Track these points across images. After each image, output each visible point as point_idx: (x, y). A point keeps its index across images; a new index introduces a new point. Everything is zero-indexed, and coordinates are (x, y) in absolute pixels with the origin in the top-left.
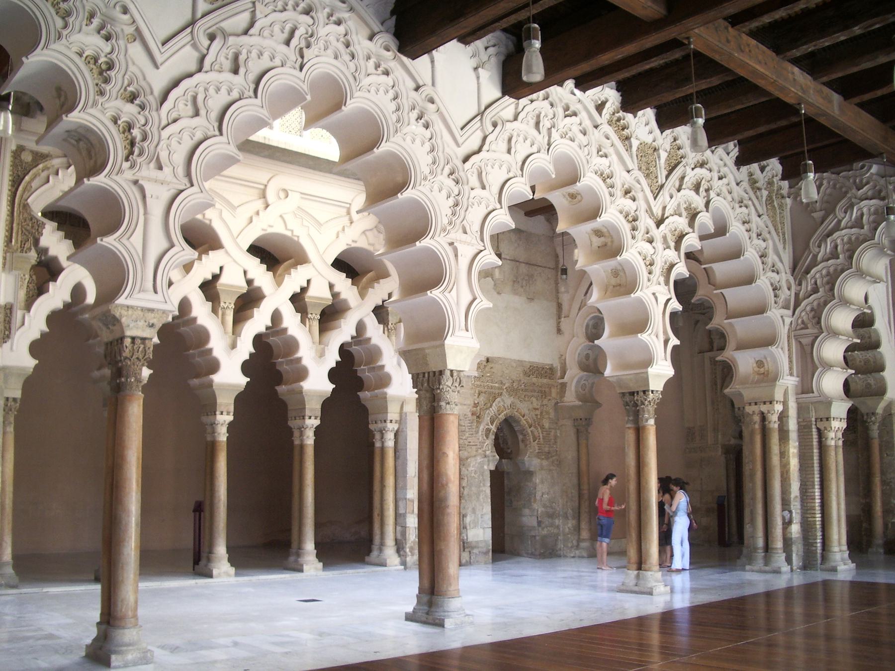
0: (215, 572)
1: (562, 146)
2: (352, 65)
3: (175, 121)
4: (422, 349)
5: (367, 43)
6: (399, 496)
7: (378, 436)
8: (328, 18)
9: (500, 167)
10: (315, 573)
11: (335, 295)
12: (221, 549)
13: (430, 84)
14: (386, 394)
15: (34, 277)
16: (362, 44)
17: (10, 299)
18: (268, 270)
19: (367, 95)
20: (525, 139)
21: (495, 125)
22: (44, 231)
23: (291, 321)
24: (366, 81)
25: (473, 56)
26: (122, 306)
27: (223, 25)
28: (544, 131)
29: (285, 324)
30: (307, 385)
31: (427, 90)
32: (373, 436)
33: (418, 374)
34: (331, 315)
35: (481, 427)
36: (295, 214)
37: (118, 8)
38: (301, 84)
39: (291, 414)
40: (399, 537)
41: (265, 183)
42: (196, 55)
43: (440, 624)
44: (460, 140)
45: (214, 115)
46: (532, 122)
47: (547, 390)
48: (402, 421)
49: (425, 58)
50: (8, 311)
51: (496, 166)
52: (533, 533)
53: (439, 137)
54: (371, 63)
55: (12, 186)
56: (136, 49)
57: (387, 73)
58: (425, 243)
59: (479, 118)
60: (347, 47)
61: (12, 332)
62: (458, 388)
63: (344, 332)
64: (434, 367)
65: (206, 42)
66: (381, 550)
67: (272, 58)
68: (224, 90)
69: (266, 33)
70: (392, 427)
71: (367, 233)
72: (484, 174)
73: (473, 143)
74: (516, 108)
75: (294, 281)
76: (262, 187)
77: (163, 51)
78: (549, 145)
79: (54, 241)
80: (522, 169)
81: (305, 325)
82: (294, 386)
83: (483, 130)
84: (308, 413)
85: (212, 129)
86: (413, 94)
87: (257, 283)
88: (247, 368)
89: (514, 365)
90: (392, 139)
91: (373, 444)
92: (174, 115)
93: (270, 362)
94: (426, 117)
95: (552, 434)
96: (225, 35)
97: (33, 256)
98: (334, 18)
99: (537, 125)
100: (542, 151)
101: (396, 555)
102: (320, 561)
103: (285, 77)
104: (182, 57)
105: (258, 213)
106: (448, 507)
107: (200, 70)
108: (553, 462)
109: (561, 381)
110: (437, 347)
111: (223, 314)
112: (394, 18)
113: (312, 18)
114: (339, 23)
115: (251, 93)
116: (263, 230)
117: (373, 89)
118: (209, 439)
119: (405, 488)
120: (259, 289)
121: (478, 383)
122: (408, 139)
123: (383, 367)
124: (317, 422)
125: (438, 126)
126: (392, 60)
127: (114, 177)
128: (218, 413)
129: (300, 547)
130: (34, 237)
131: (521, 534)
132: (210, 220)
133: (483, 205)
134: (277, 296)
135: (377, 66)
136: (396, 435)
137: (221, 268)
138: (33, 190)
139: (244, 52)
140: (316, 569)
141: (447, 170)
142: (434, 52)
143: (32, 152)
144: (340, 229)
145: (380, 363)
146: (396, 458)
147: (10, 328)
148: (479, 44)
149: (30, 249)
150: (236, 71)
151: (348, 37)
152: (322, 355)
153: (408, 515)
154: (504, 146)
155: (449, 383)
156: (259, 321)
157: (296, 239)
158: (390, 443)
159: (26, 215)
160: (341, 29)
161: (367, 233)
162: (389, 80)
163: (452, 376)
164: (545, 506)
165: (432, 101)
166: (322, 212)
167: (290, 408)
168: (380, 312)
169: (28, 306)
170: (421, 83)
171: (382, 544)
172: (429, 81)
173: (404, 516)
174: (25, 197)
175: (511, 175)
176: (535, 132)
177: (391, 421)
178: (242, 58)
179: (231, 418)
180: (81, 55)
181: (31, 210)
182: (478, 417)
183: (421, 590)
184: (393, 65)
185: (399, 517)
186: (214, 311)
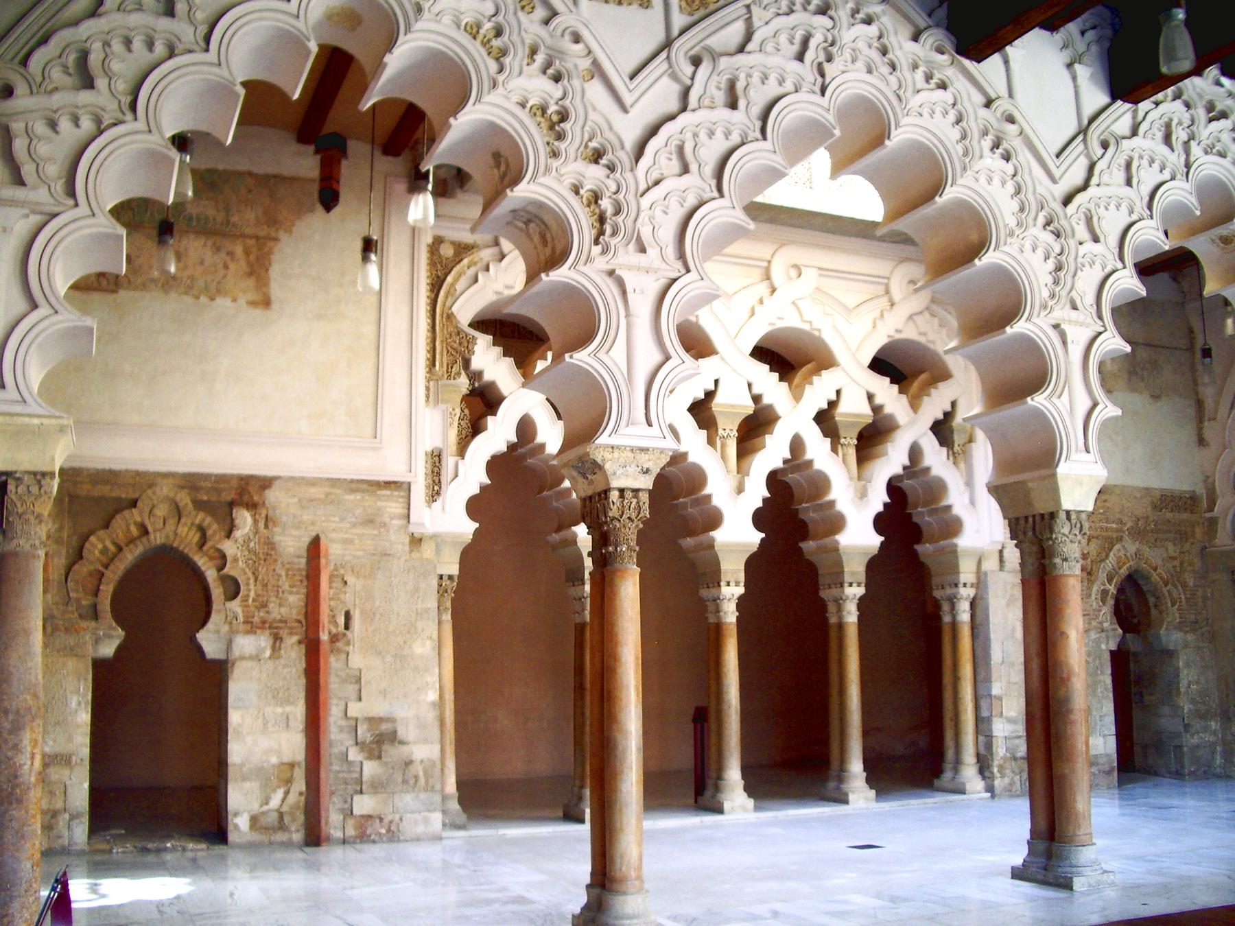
1: (1208, 166)
2: (893, 80)
3: (657, 183)
4: (1023, 483)
5: (911, 46)
6: (981, 691)
7: (946, 607)
8: (853, 16)
9: (1118, 207)
11: (877, 409)
12: (734, 774)
13: (1006, 95)
14: (955, 545)
15: (467, 411)
16: (905, 49)
17: (438, 443)
18: (781, 380)
19: (918, 121)
20: (1152, 162)
21: (1105, 145)
22: (476, 348)
23: (818, 450)
24: (915, 101)
25: (1065, 47)
26: (606, 446)
27: (708, 42)
28: (1178, 146)
31: (1003, 105)
33: (1017, 519)
35: (1095, 589)
37: (567, 37)
38: (826, 115)
40: (982, 751)
42: (676, 89)
43: (1066, 885)
44: (1057, 173)
45: (709, 170)
46: (1159, 135)
47: (1189, 530)
48: (980, 583)
49: (996, 58)
51: (1112, 207)
52: (1177, 742)
53: (1026, 171)
54: (919, 75)
55: (432, 291)
56: (595, 90)
57: (943, 86)
58: (1019, 327)
59: (1080, 138)
60: (884, 54)
63: (892, 461)
64: (1041, 507)
65: (689, 69)
67: (781, 82)
68: (719, 134)
69: (769, 47)
70: (966, 593)
71: (916, 318)
72: (1095, 219)
73: (1076, 175)
74: (1134, 118)
75: (818, 392)
76: (765, 264)
77: (631, 87)
78: (1188, 166)
79: (490, 361)
80: (1150, 207)
81: (837, 453)
82: (827, 540)
83: (1088, 156)
84: (847, 578)
85: (708, 189)
86: (983, 113)
87: (766, 400)
88: (760, 519)
89: (1138, 495)
90: (960, 181)
92: (655, 175)
93: (791, 511)
94: (1005, 145)
95: (1200, 593)
96: (715, 56)
97: (463, 383)
98: (860, 16)
99: (1167, 139)
100: (1179, 176)
102: (871, 788)
103: (800, 108)
104: (657, 94)
105: (761, 302)
107: (684, 109)
108: (1203, 635)
109: (1208, 515)
110: (1043, 478)
111: (723, 446)
112: (945, 6)
113: (831, 18)
114: (868, 21)
115: (758, 135)
117: (926, 112)
118: (712, 620)
119: (988, 679)
120: (770, 407)
122: (983, 179)
123: (949, 507)
125: (1024, 156)
126: (947, 65)
127: (580, 267)
128: (723, 584)
129: (842, 768)
131: (1159, 744)
133: (1098, 266)
134: (795, 415)
135: (928, 77)
136: (973, 604)
137: (716, 382)
138: (458, 293)
139: (742, 76)
140: (867, 799)
141: (1041, 220)
142: (1008, 48)
143: (453, 243)
144: (877, 313)
145: (945, 503)
148: (1072, 28)
149: (459, 374)
150: (733, 105)
151: (884, 40)
152: (863, 494)
153: (995, 719)
154: (1120, 176)
155: (1066, 530)
156: (772, 453)
158: (964, 616)
160: (873, 30)
162: (946, 96)
164: (1193, 701)
165: (1011, 120)
169: (462, 451)
170: (993, 96)
171: (958, 762)
172: (1003, 92)
173: (989, 720)
174: (448, 304)
175: (1135, 217)
176: (1165, 150)
177: (965, 585)
178: (740, 86)
179: (741, 590)
180: (523, 106)
182: (1089, 574)
183: (1033, 832)
184: (951, 73)
185: (982, 724)
186: (711, 441)
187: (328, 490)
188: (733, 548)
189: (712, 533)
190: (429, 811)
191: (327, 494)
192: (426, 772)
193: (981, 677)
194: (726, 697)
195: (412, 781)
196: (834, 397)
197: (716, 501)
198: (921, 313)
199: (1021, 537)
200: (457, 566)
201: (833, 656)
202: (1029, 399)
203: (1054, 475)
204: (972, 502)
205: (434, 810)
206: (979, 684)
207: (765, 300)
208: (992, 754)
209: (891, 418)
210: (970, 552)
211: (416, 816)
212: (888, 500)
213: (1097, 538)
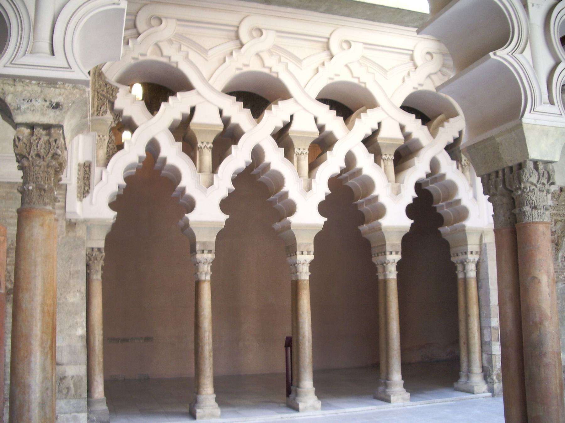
0: (301, 406)
4: (492, 138)
6: (483, 325)
7: (460, 268)
10: (401, 404)
11: (407, 136)
12: (307, 383)
14: (464, 226)
17: (88, 158)
18: (337, 115)
22: (118, 95)
23: (365, 162)
29: (359, 165)
30: (385, 222)
32: (455, 268)
33: (489, 175)
34: (404, 156)
36: (360, 64)
39: (374, 251)
40: (485, 364)
41: (328, 36)
48: (482, 251)
50: (87, 169)
61: (91, 187)
62: (547, 186)
63: (418, 170)
64: (509, 160)
66: (468, 377)
70: (472, 258)
71: (432, 77)
75: (364, 124)
76: (325, 40)
81: (379, 164)
82: (374, 223)
84: (388, 249)
88: (323, 208)
91: (456, 275)
93: (347, 202)
101: (484, 382)
102: (407, 391)
105: (323, 64)
106: (545, 355)
110: (510, 131)
111: (298, 160)
116: (330, 79)
118: (294, 279)
119: (489, 317)
120: (331, 134)
121: (555, 212)
123: (459, 201)
124: (398, 257)
128: (298, 253)
129: (387, 378)
130: (109, 101)
132: (277, 73)
134: (349, 139)
136: (477, 265)
137: (292, 117)
140: (404, 399)
144: (405, 73)
145: (457, 198)
146: (478, 287)
147: (89, 184)
149: (106, 112)
152: (398, 192)
153: (493, 343)
155: (534, 179)
156: (333, 163)
157: (363, 85)
158: (472, 274)
159: (101, 82)
161: (432, 77)
163: (536, 167)
166: (385, 60)
167: (372, 246)
168: (452, 149)
173: (490, 343)
177: (472, 253)
179: (311, 257)
181: (106, 78)
182: (557, 245)
187: (8, 190)
188: (305, 228)
189: (289, 218)
190: (78, 412)
191: (8, 193)
192: (75, 384)
193: (484, 314)
194: (301, 331)
195: (65, 391)
196: (376, 127)
197: (291, 196)
198: (436, 73)
199: (493, 191)
200: (103, 242)
201: (381, 300)
202: (491, 54)
203: (520, 125)
204: (475, 197)
205: (82, 412)
206: (482, 319)
207: (325, 63)
208: (492, 367)
209: (417, 141)
210: (475, 231)
211: (68, 416)
212: (416, 196)
213: (561, 221)
